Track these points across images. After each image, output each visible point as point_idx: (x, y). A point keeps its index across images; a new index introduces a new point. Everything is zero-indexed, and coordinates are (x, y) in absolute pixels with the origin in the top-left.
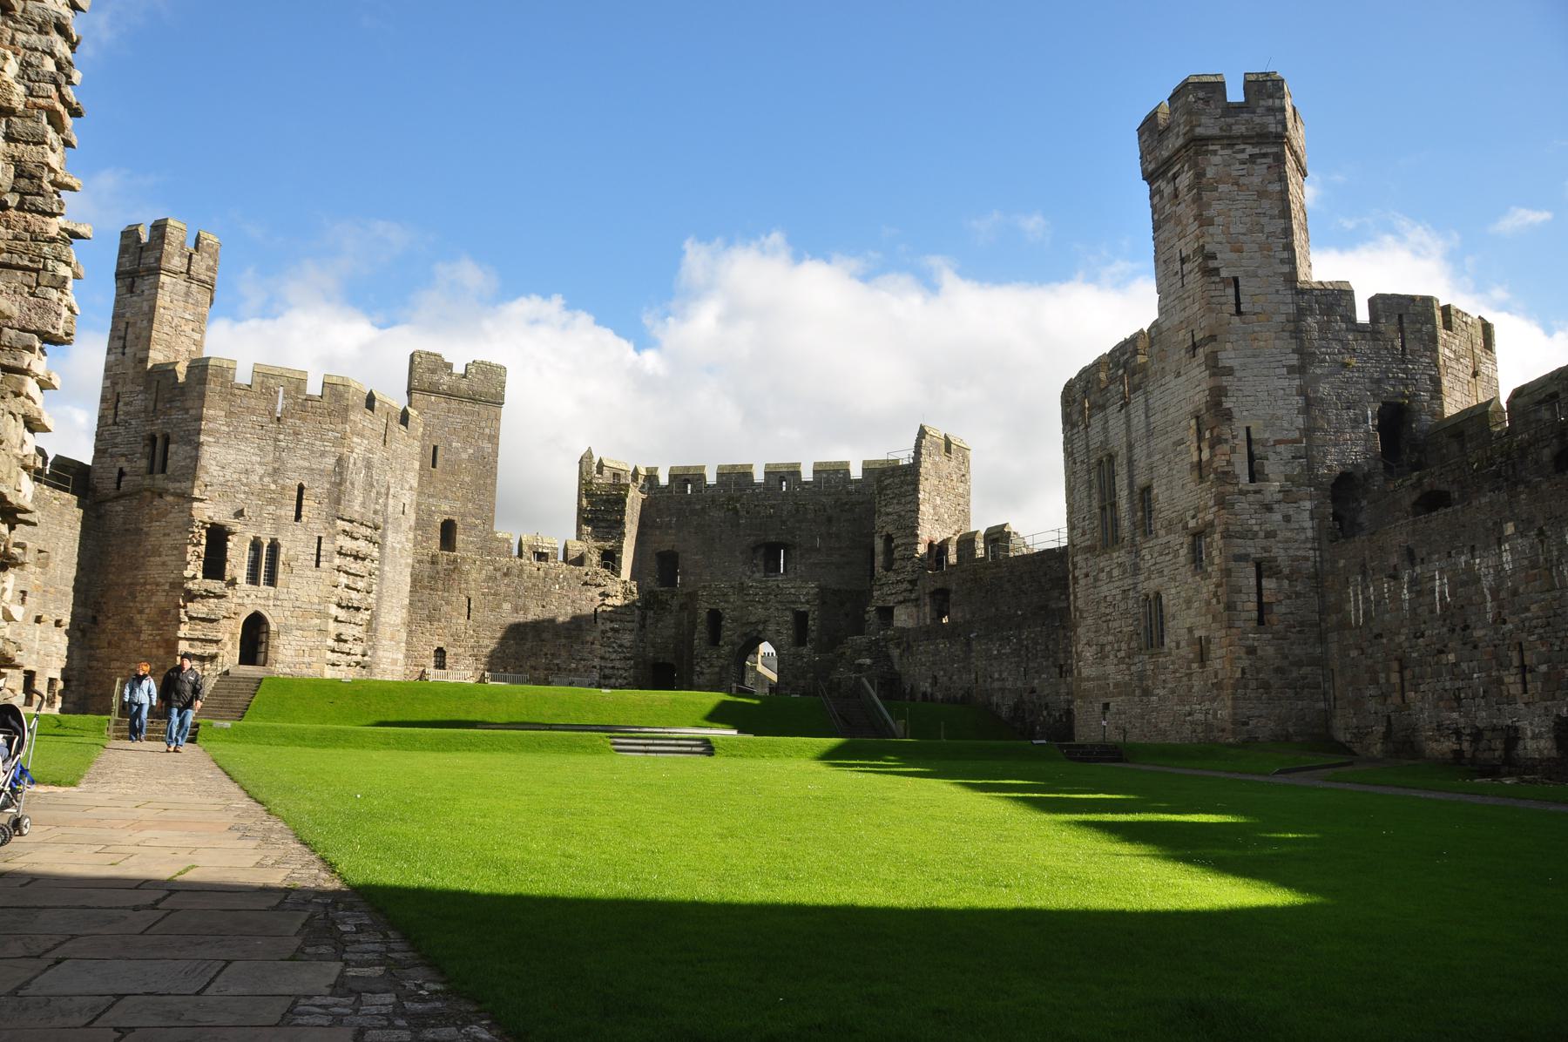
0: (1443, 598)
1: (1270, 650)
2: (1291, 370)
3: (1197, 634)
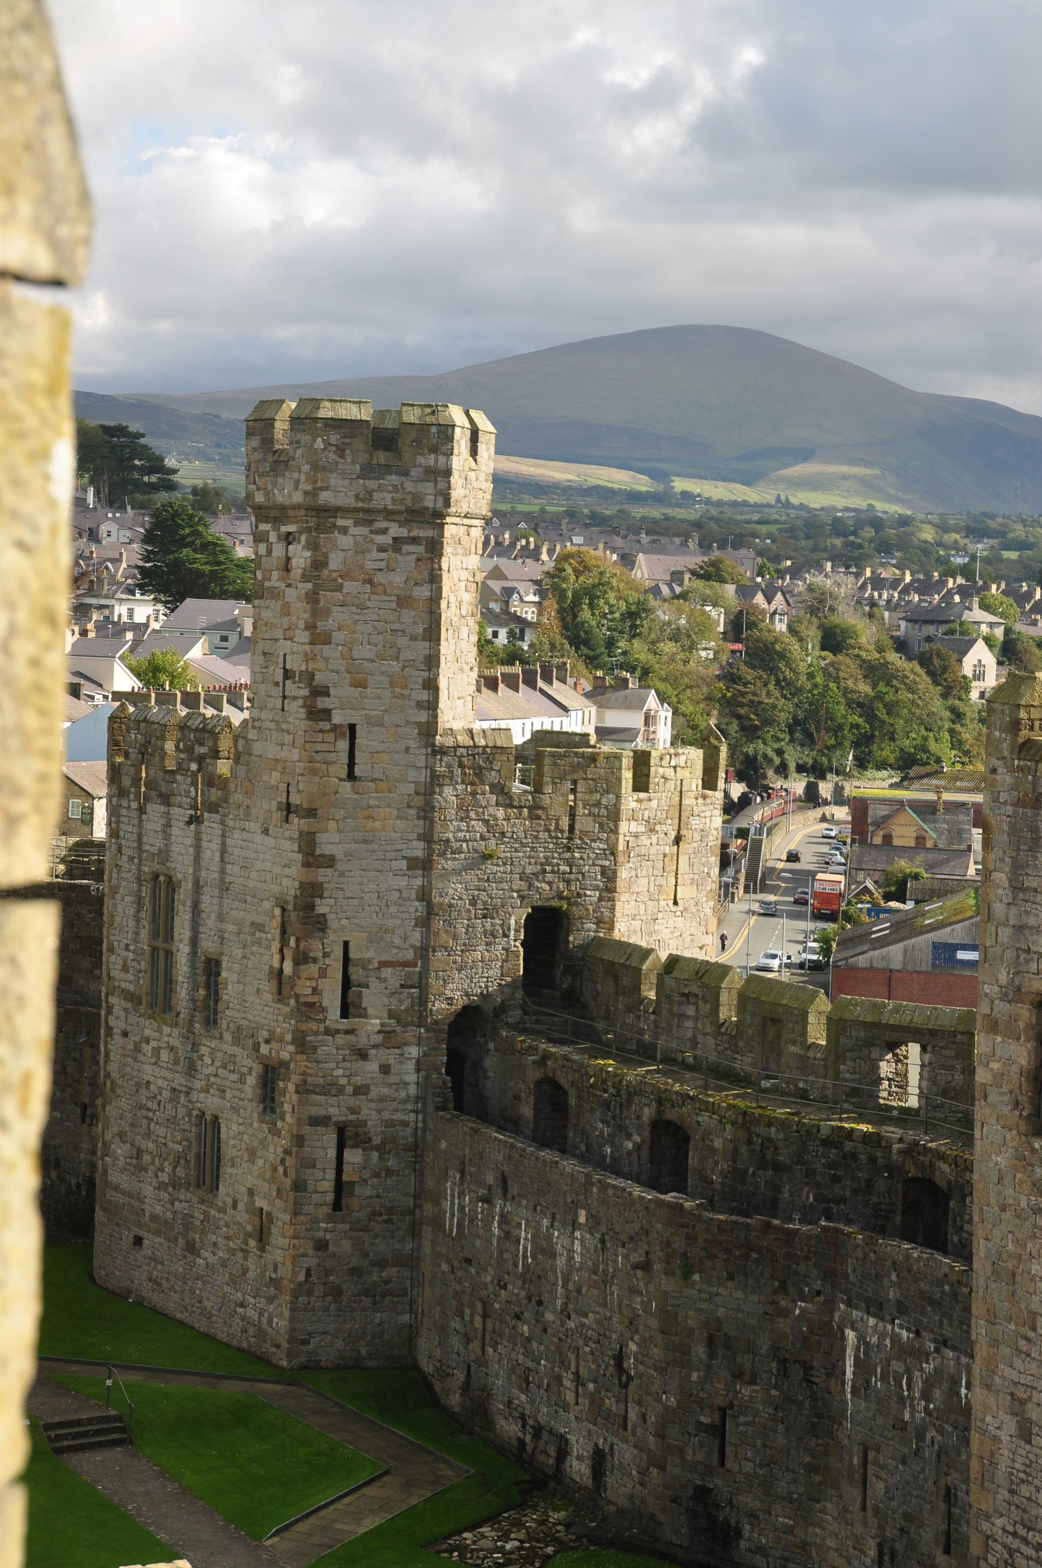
0: (525, 1257)
1: (347, 1245)
2: (413, 864)
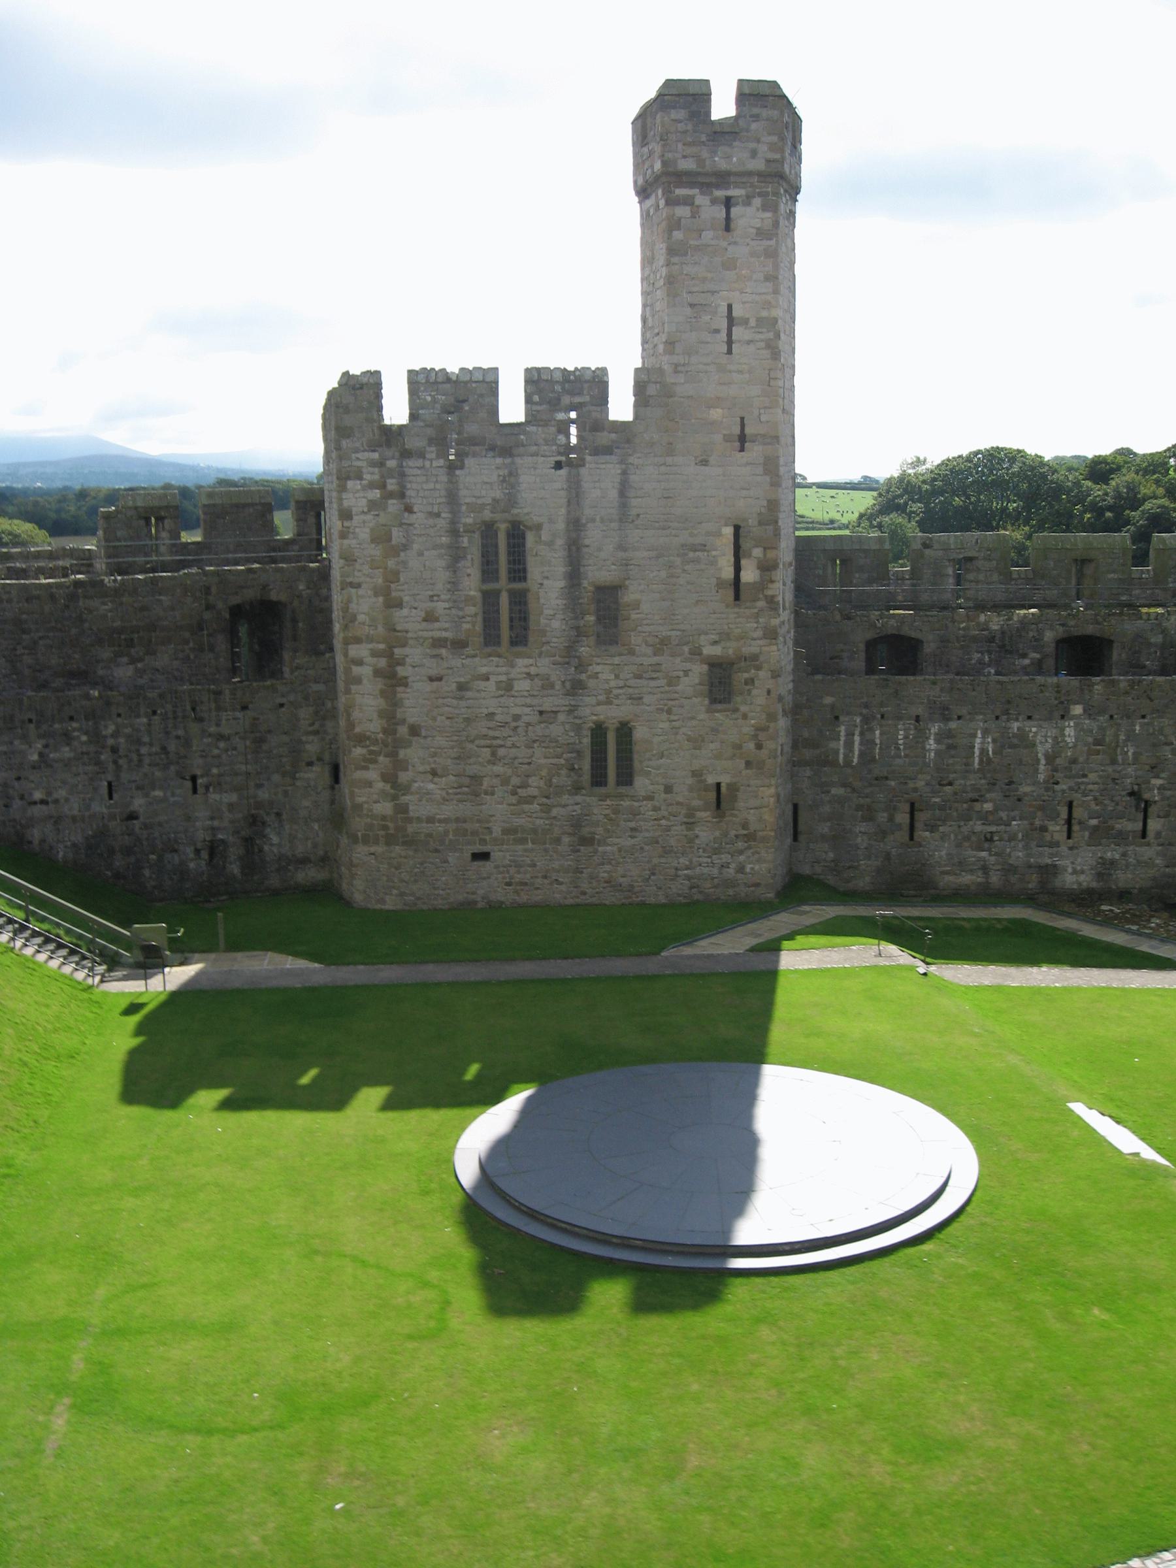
3: (711, 780)
